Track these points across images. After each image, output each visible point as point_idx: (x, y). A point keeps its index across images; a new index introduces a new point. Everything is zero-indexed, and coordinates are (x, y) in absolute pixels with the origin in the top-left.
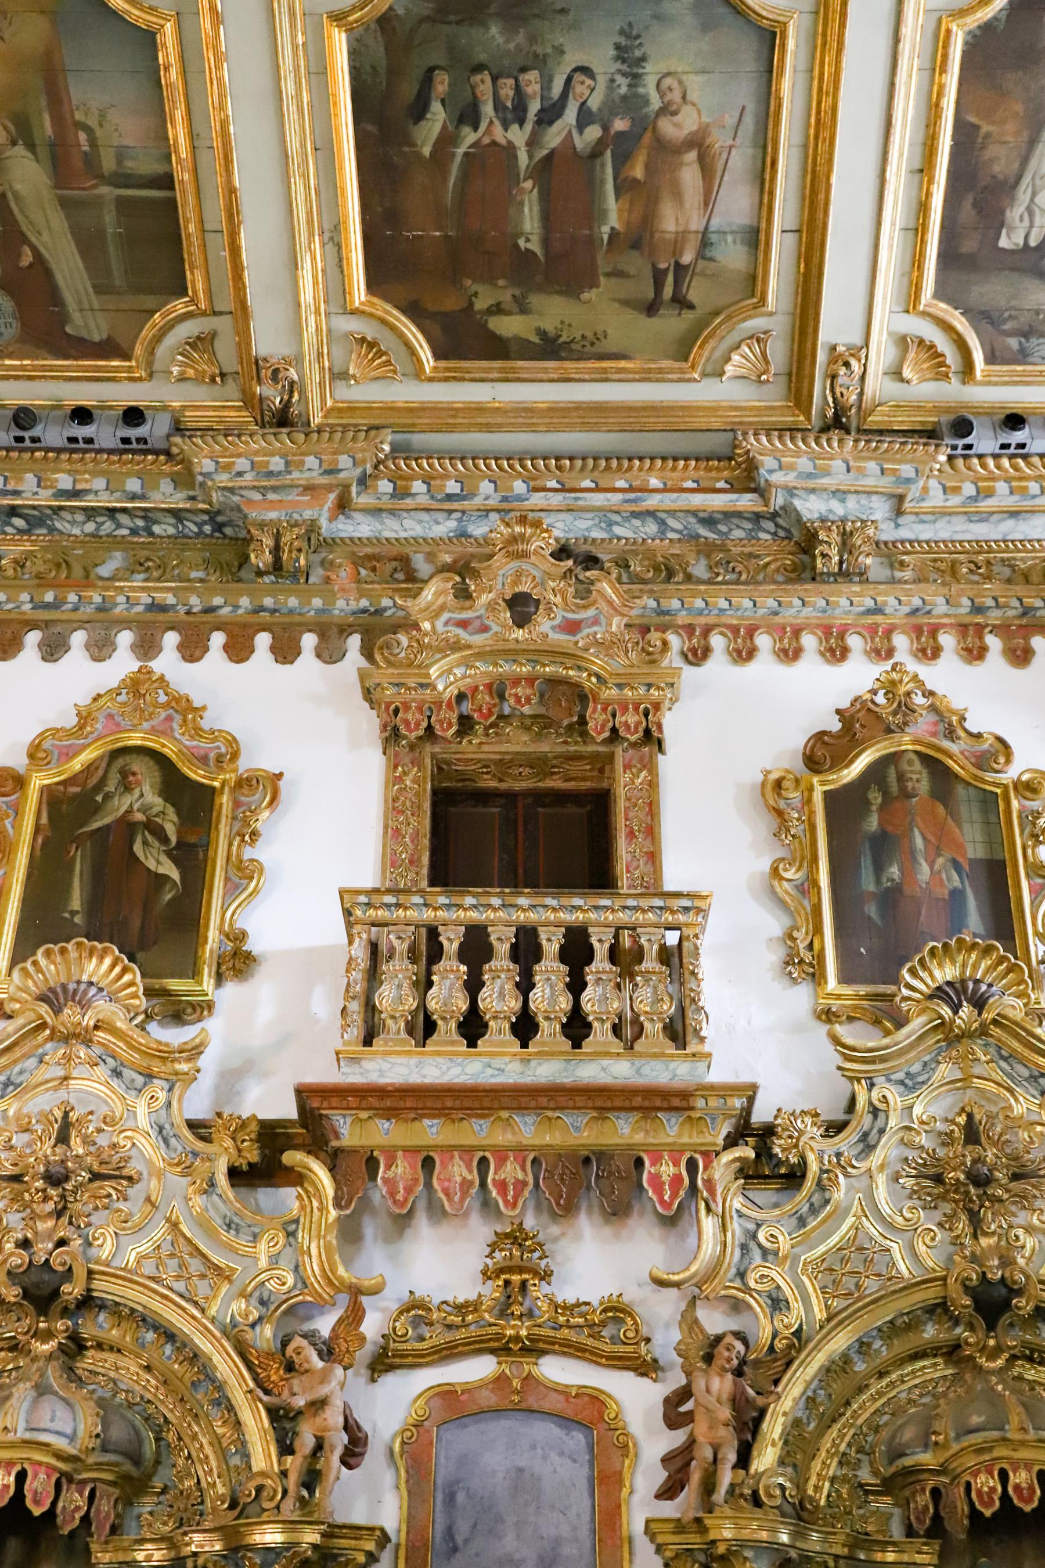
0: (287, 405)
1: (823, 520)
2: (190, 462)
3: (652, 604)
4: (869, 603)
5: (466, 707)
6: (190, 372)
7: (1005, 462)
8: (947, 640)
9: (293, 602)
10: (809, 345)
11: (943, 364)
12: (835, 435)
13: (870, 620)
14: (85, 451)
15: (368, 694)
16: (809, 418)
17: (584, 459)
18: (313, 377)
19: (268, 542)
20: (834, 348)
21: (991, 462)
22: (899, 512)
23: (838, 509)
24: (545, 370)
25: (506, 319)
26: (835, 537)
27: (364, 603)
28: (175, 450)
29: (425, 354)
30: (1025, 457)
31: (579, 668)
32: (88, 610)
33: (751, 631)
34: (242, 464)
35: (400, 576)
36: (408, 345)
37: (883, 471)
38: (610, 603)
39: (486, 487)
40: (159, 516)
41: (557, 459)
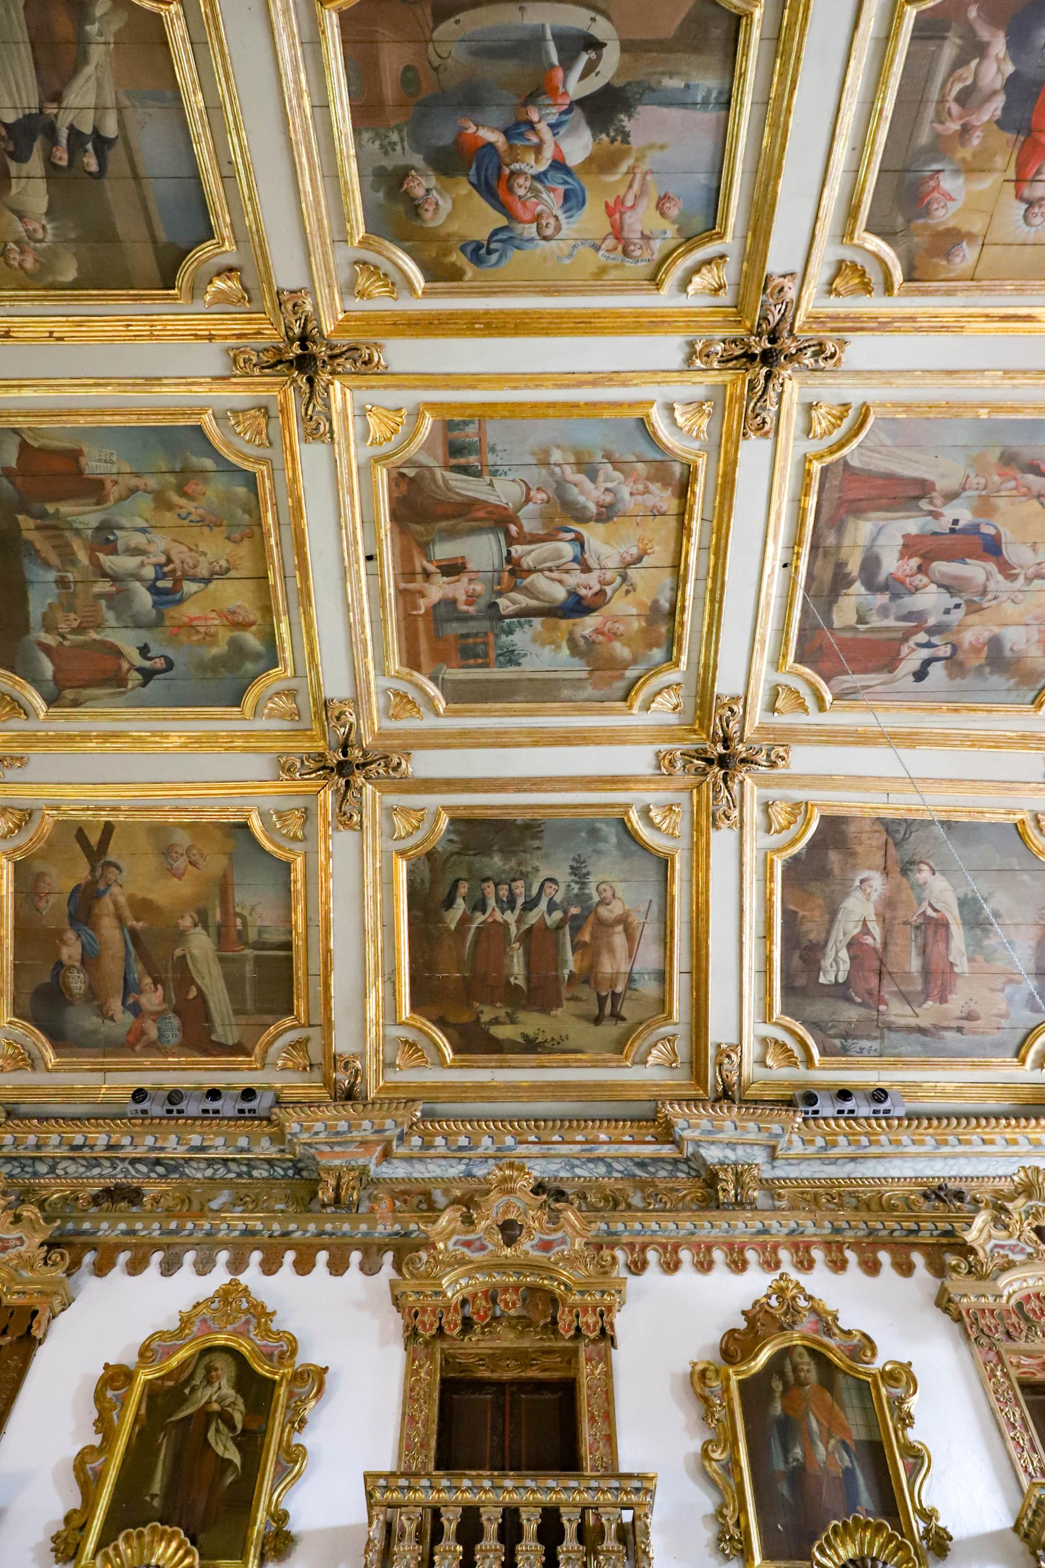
0: (353, 1085)
1: (722, 1164)
2: (283, 1126)
3: (604, 1227)
4: (759, 1226)
5: (469, 1310)
6: (290, 1064)
7: (842, 1123)
8: (817, 1254)
9: (346, 1227)
10: (702, 1043)
11: (792, 1056)
12: (725, 1104)
13: (761, 1238)
14: (213, 1119)
15: (396, 1300)
16: (706, 1092)
17: (554, 1121)
18: (371, 1065)
19: (332, 1182)
20: (719, 1046)
21: (832, 1123)
22: (773, 1157)
23: (732, 1156)
24: (528, 1061)
25: (500, 1027)
26: (731, 1177)
27: (397, 1227)
28: (274, 1117)
29: (448, 1051)
30: (855, 1119)
31: (552, 1278)
32: (199, 1235)
33: (676, 1248)
34: (319, 1126)
35: (424, 1206)
36: (436, 1044)
37: (759, 1129)
38: (573, 1227)
39: (486, 1141)
40: (258, 1163)
41: (536, 1121)
